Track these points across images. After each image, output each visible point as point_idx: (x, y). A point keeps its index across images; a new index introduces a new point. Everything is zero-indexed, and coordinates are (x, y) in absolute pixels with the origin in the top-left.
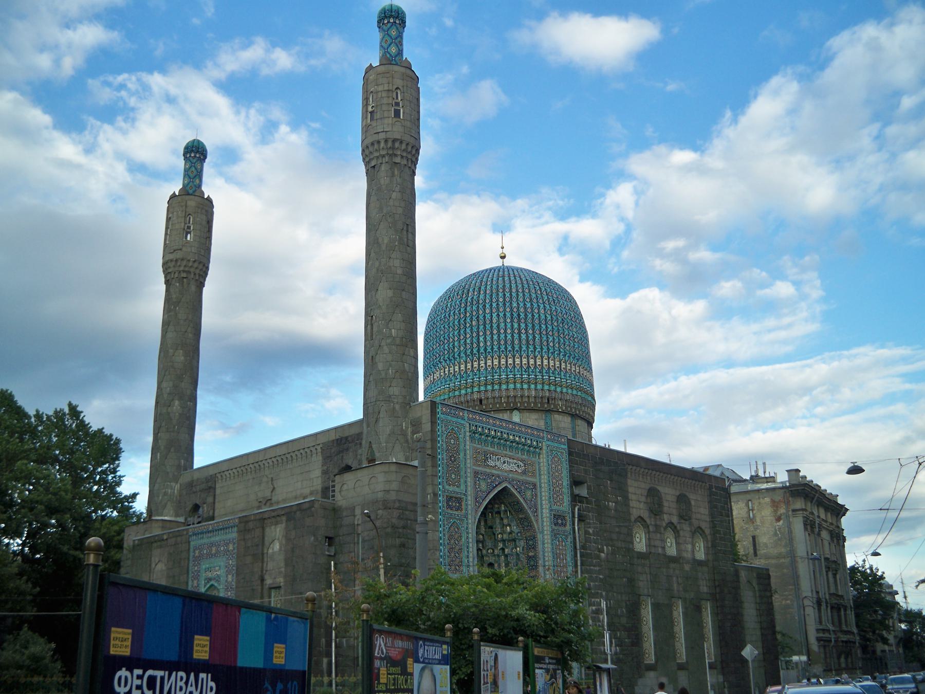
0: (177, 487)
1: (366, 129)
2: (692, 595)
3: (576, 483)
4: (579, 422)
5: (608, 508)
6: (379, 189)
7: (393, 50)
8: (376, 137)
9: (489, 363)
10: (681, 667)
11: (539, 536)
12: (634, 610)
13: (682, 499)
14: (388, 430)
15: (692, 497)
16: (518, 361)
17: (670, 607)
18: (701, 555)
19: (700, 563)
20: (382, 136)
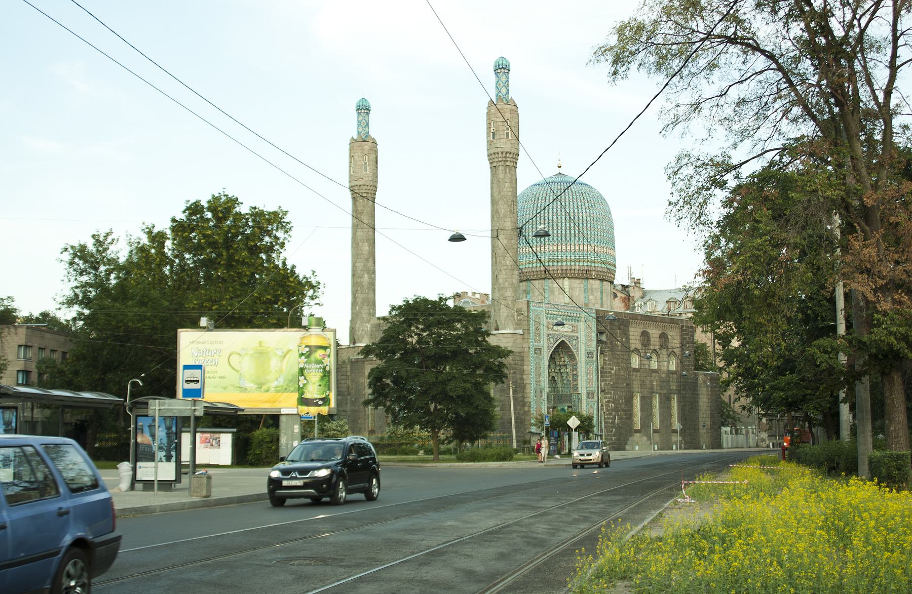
0: (369, 326)
1: (490, 143)
2: (665, 391)
3: (600, 333)
4: (605, 283)
5: (617, 345)
6: (498, 181)
7: (504, 91)
8: (496, 150)
9: (551, 248)
10: (655, 431)
11: (579, 364)
12: (629, 401)
13: (663, 336)
14: (505, 314)
15: (670, 334)
16: (568, 247)
17: (651, 398)
18: (673, 368)
19: (672, 372)
20: (500, 150)
